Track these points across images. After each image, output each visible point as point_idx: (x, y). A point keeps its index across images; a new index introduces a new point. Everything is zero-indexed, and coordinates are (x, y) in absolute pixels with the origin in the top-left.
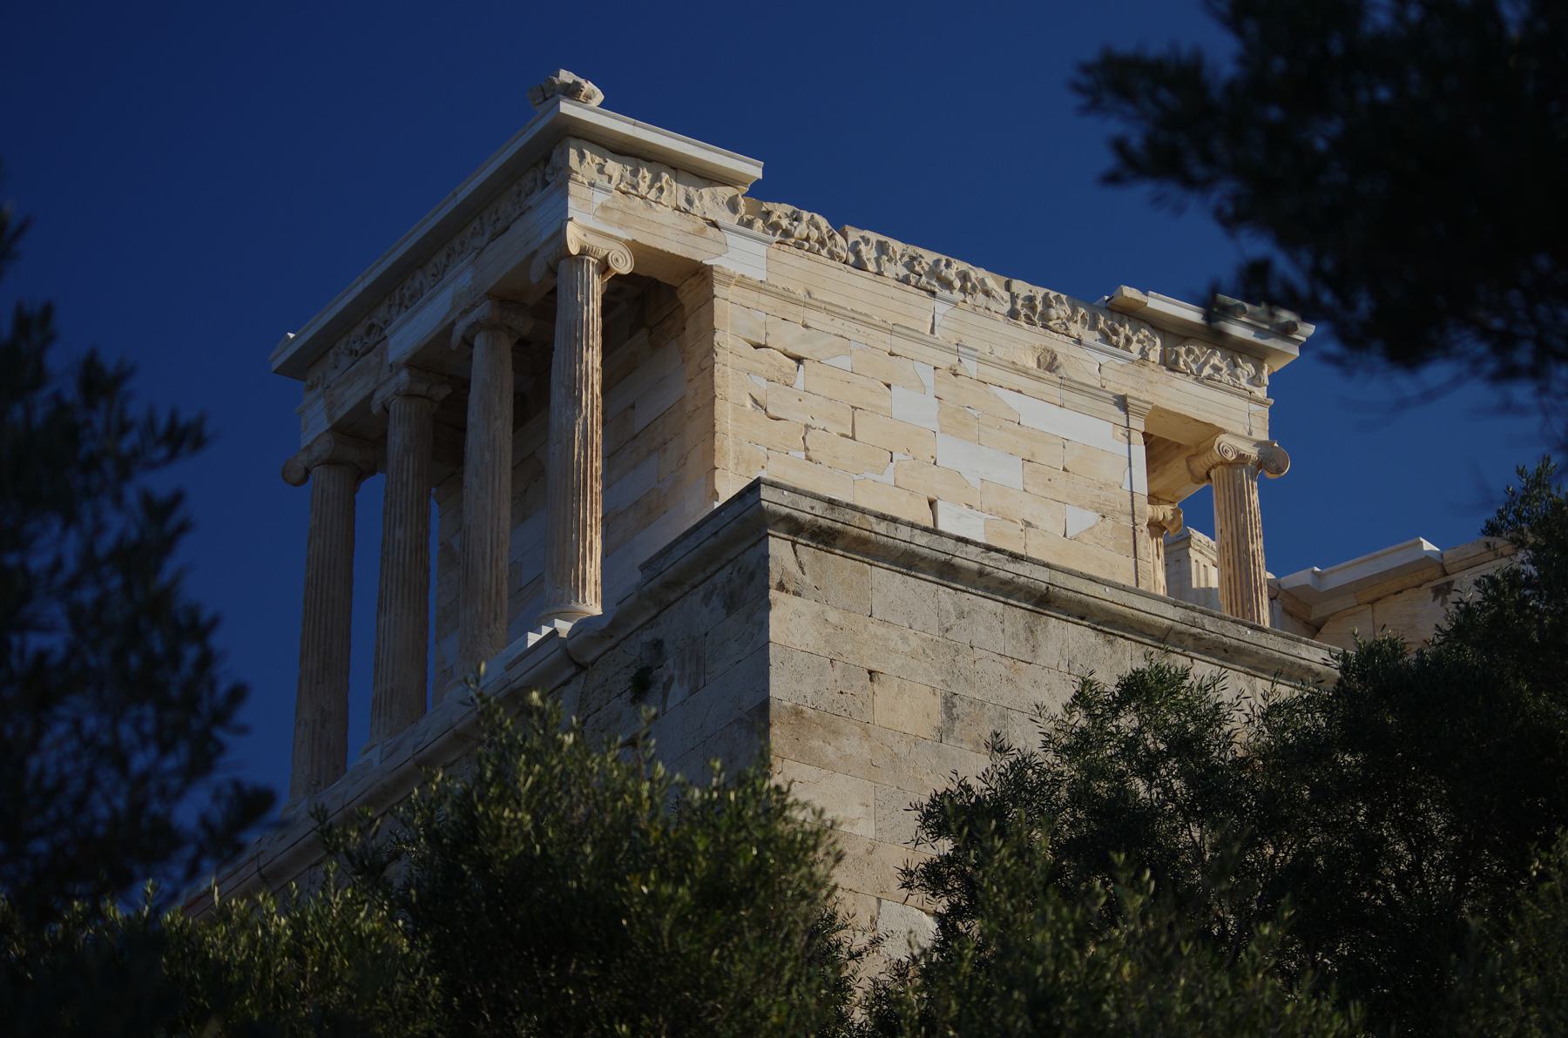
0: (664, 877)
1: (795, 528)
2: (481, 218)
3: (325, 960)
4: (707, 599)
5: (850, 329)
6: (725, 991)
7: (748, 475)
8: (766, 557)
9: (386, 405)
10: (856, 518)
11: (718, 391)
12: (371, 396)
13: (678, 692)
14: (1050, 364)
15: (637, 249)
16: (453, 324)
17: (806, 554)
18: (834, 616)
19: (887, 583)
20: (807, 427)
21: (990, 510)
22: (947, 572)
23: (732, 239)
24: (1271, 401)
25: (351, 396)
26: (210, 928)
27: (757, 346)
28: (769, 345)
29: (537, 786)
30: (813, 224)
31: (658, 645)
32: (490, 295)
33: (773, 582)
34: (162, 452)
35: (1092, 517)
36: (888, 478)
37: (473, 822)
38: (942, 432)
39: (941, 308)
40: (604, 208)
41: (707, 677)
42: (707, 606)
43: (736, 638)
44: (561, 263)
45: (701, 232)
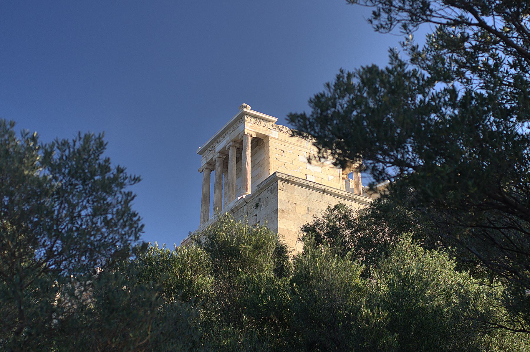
0: (247, 244)
1: (282, 179)
3: (192, 258)
4: (268, 191)
5: (292, 146)
6: (258, 263)
13: (263, 207)
15: (256, 132)
17: (284, 184)
18: (289, 194)
19: (297, 188)
22: (308, 187)
23: (272, 131)
25: (210, 158)
29: (227, 228)
31: (260, 199)
33: (279, 189)
34: (133, 182)
35: (333, 177)
36: (299, 171)
37: (216, 235)
40: (251, 126)
44: (244, 135)
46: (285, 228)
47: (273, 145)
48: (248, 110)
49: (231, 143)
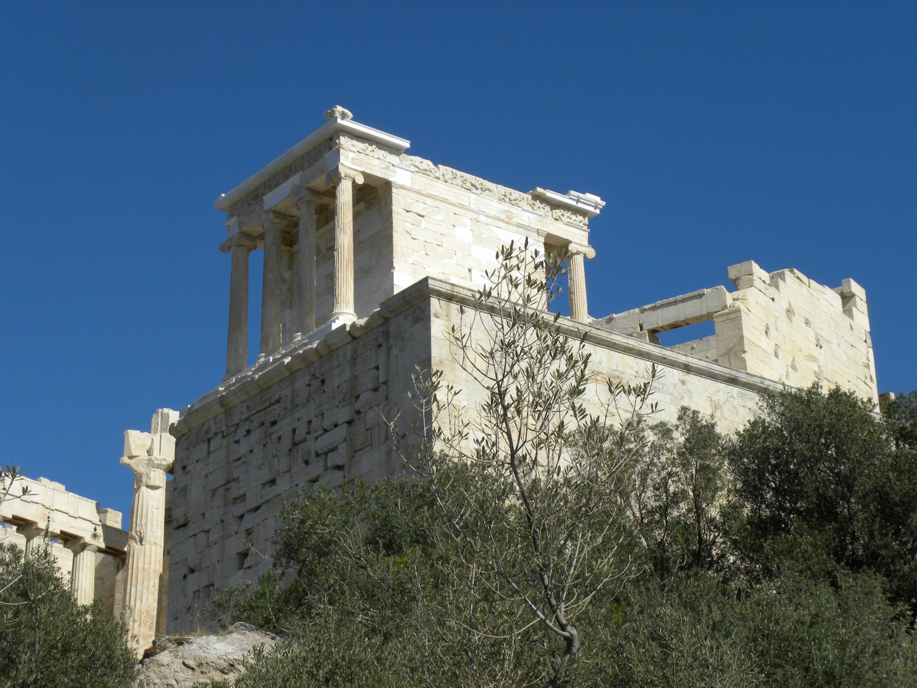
1: (440, 295)
4: (405, 318)
5: (440, 204)
8: (429, 304)
10: (461, 290)
11: (394, 229)
14: (509, 215)
15: (364, 174)
17: (443, 303)
23: (397, 170)
24: (589, 230)
27: (408, 212)
30: (427, 164)
39: (473, 196)
40: (353, 159)
44: (335, 177)
45: (388, 168)
47: (399, 201)
48: (344, 118)
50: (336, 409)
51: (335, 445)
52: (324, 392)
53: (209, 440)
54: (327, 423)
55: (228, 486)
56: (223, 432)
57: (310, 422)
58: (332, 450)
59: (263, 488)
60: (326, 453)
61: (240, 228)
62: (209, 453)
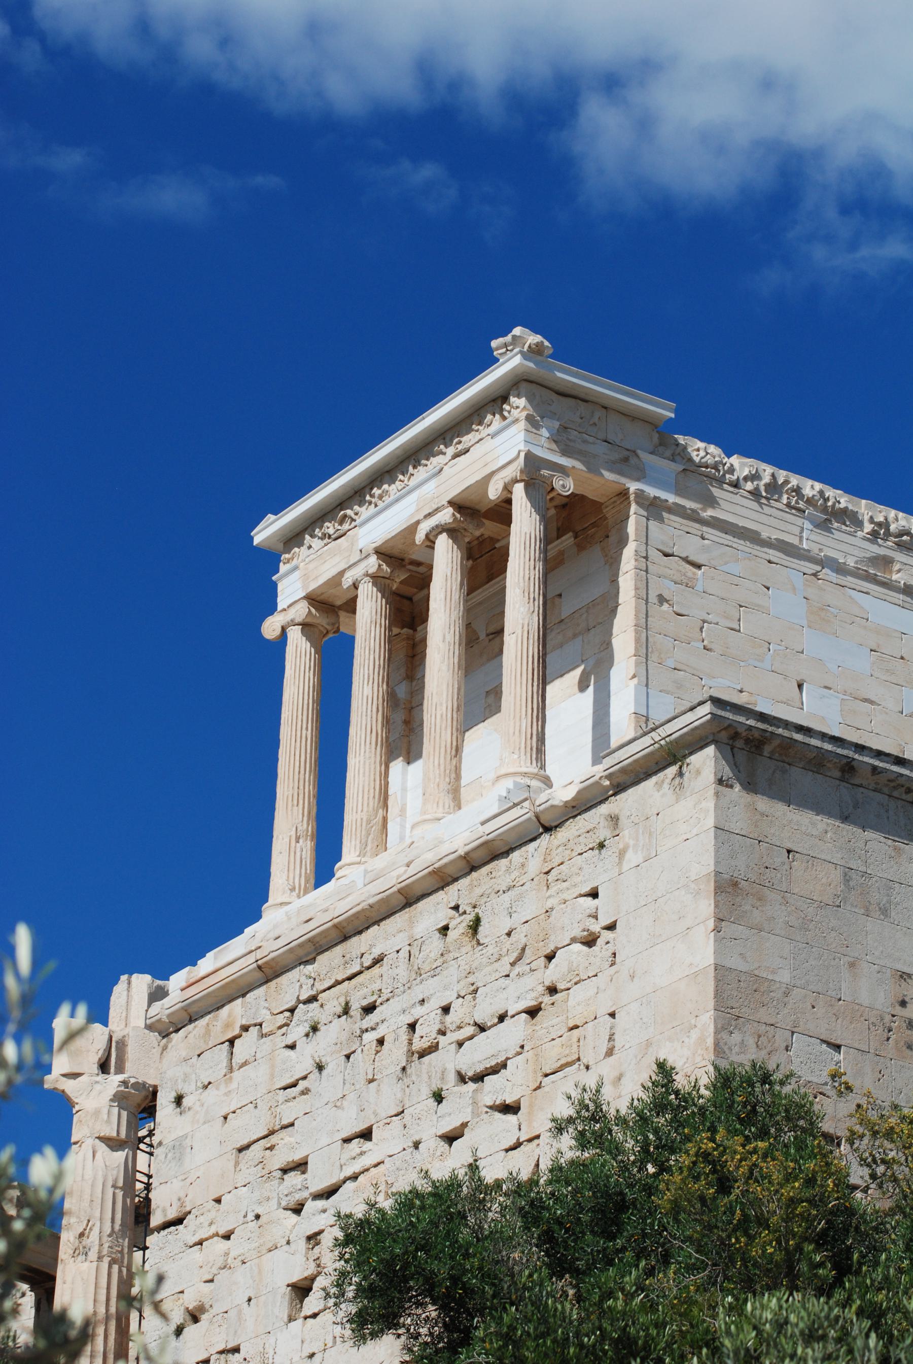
2: (444, 439)
7: (659, 661)
9: (357, 584)
12: (342, 573)
13: (632, 858)
16: (418, 523)
20: (704, 621)
21: (845, 692)
26: (711, 1232)
27: (666, 555)
28: (675, 554)
32: (451, 503)
38: (809, 627)
41: (659, 849)
42: (658, 791)
43: (684, 820)
46: (743, 967)
49: (446, 516)
50: (504, 982)
51: (500, 1059)
52: (479, 944)
53: (231, 1042)
54: (485, 1012)
55: (273, 1139)
56: (261, 1025)
57: (446, 1010)
58: (495, 1070)
59: (342, 1148)
60: (479, 1078)
61: (304, 586)
62: (231, 1069)
